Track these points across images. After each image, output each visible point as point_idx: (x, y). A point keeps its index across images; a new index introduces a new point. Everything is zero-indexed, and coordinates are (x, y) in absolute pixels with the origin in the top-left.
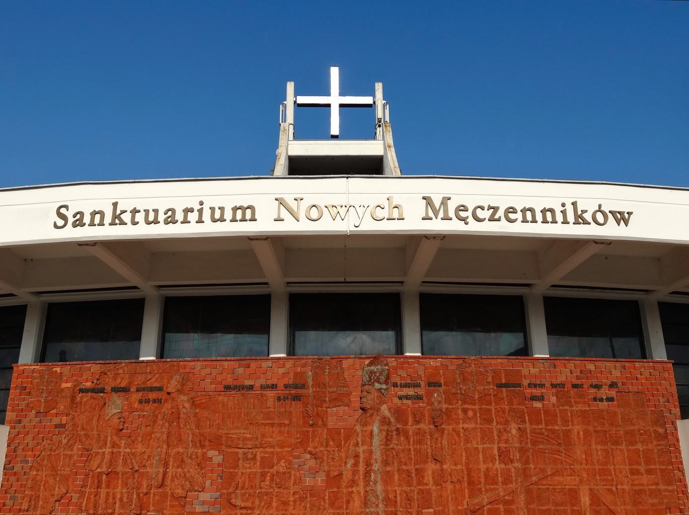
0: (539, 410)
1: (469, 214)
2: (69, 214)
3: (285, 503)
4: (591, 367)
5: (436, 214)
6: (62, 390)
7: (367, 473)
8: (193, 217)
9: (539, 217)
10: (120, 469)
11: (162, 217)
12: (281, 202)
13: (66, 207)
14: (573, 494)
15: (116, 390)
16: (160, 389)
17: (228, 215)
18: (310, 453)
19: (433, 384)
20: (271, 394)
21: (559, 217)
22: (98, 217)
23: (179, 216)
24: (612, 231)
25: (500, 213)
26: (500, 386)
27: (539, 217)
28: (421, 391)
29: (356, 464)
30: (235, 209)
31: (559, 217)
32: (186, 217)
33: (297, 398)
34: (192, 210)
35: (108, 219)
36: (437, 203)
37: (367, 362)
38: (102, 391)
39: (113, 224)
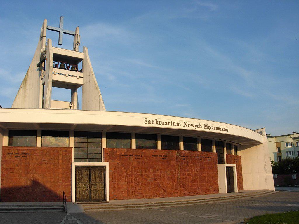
2: (148, 121)
3: (165, 180)
6: (117, 155)
7: (178, 174)
8: (170, 124)
10: (134, 173)
11: (165, 124)
12: (184, 123)
13: (147, 119)
14: (205, 177)
15: (130, 155)
16: (140, 156)
17: (176, 125)
18: (168, 170)
20: (161, 158)
22: (153, 122)
23: (168, 124)
29: (176, 172)
30: (177, 123)
32: (169, 124)
33: (165, 159)
34: (170, 123)
35: (155, 123)
36: (206, 125)
37: (177, 151)
38: (127, 155)
39: (156, 124)
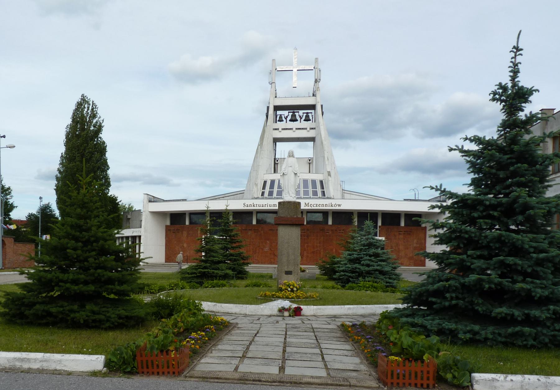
0: (327, 235)
1: (312, 206)
2: (246, 205)
4: (339, 226)
5: (307, 205)
8: (266, 206)
9: (324, 206)
11: (261, 206)
15: (249, 230)
16: (257, 230)
17: (272, 206)
19: (308, 230)
21: (328, 206)
23: (264, 206)
24: (338, 208)
25: (318, 205)
26: (321, 230)
27: (324, 206)
28: (305, 231)
31: (328, 206)
35: (252, 206)
36: (307, 204)
